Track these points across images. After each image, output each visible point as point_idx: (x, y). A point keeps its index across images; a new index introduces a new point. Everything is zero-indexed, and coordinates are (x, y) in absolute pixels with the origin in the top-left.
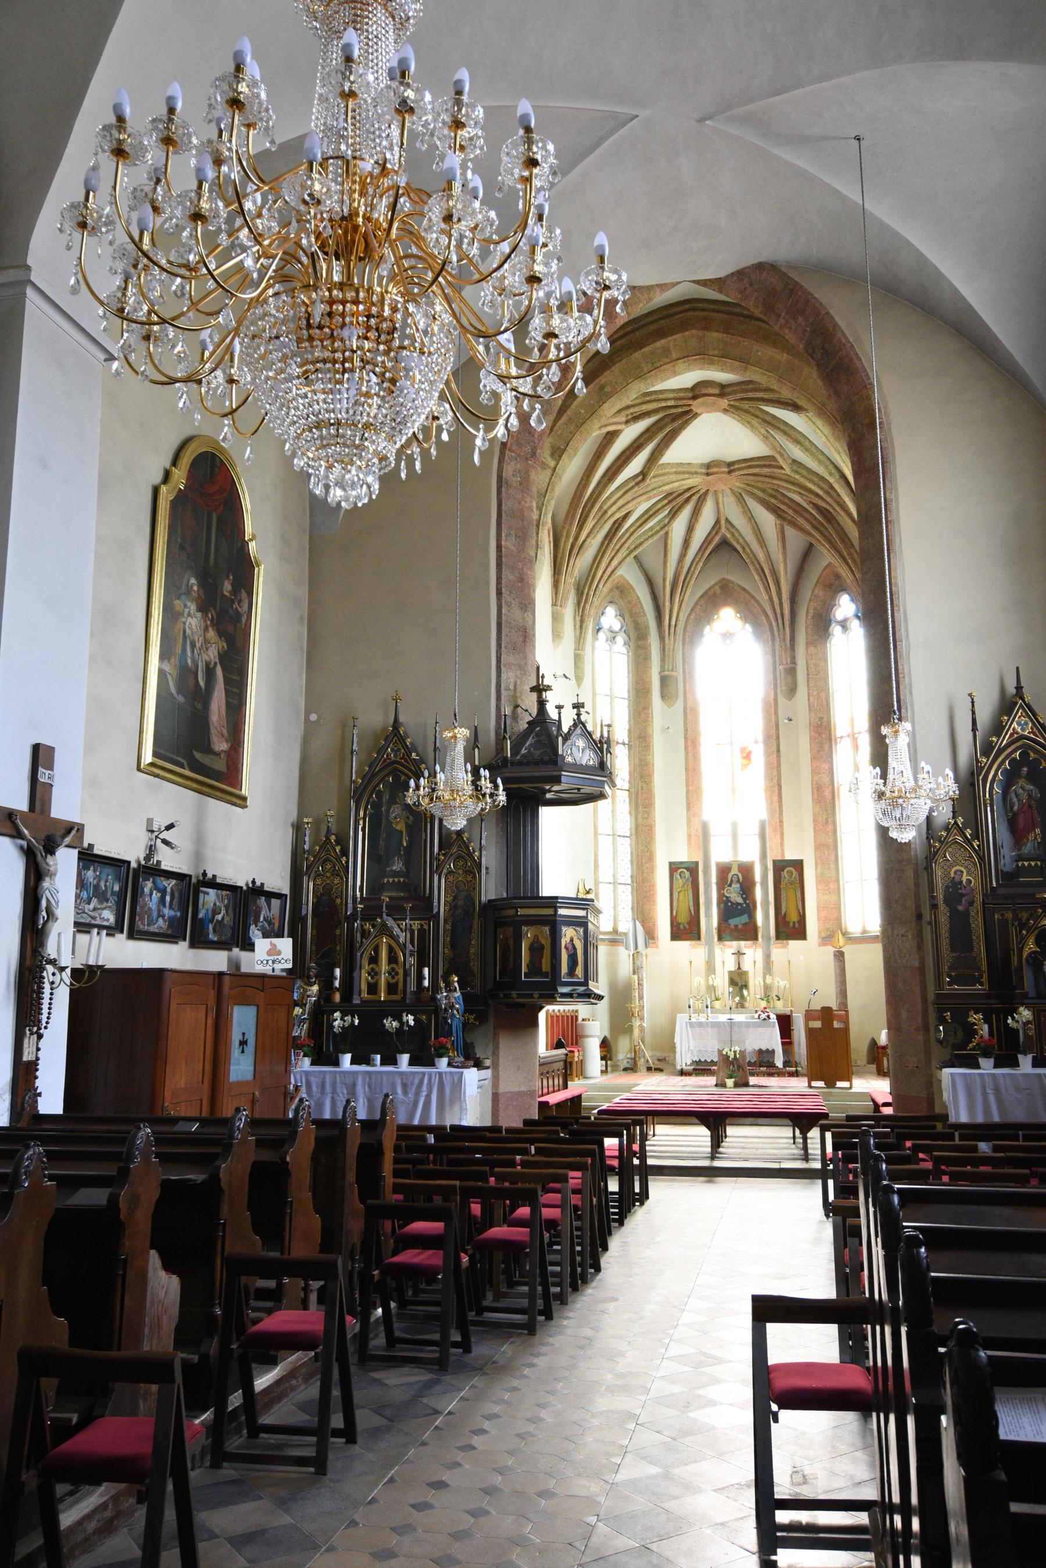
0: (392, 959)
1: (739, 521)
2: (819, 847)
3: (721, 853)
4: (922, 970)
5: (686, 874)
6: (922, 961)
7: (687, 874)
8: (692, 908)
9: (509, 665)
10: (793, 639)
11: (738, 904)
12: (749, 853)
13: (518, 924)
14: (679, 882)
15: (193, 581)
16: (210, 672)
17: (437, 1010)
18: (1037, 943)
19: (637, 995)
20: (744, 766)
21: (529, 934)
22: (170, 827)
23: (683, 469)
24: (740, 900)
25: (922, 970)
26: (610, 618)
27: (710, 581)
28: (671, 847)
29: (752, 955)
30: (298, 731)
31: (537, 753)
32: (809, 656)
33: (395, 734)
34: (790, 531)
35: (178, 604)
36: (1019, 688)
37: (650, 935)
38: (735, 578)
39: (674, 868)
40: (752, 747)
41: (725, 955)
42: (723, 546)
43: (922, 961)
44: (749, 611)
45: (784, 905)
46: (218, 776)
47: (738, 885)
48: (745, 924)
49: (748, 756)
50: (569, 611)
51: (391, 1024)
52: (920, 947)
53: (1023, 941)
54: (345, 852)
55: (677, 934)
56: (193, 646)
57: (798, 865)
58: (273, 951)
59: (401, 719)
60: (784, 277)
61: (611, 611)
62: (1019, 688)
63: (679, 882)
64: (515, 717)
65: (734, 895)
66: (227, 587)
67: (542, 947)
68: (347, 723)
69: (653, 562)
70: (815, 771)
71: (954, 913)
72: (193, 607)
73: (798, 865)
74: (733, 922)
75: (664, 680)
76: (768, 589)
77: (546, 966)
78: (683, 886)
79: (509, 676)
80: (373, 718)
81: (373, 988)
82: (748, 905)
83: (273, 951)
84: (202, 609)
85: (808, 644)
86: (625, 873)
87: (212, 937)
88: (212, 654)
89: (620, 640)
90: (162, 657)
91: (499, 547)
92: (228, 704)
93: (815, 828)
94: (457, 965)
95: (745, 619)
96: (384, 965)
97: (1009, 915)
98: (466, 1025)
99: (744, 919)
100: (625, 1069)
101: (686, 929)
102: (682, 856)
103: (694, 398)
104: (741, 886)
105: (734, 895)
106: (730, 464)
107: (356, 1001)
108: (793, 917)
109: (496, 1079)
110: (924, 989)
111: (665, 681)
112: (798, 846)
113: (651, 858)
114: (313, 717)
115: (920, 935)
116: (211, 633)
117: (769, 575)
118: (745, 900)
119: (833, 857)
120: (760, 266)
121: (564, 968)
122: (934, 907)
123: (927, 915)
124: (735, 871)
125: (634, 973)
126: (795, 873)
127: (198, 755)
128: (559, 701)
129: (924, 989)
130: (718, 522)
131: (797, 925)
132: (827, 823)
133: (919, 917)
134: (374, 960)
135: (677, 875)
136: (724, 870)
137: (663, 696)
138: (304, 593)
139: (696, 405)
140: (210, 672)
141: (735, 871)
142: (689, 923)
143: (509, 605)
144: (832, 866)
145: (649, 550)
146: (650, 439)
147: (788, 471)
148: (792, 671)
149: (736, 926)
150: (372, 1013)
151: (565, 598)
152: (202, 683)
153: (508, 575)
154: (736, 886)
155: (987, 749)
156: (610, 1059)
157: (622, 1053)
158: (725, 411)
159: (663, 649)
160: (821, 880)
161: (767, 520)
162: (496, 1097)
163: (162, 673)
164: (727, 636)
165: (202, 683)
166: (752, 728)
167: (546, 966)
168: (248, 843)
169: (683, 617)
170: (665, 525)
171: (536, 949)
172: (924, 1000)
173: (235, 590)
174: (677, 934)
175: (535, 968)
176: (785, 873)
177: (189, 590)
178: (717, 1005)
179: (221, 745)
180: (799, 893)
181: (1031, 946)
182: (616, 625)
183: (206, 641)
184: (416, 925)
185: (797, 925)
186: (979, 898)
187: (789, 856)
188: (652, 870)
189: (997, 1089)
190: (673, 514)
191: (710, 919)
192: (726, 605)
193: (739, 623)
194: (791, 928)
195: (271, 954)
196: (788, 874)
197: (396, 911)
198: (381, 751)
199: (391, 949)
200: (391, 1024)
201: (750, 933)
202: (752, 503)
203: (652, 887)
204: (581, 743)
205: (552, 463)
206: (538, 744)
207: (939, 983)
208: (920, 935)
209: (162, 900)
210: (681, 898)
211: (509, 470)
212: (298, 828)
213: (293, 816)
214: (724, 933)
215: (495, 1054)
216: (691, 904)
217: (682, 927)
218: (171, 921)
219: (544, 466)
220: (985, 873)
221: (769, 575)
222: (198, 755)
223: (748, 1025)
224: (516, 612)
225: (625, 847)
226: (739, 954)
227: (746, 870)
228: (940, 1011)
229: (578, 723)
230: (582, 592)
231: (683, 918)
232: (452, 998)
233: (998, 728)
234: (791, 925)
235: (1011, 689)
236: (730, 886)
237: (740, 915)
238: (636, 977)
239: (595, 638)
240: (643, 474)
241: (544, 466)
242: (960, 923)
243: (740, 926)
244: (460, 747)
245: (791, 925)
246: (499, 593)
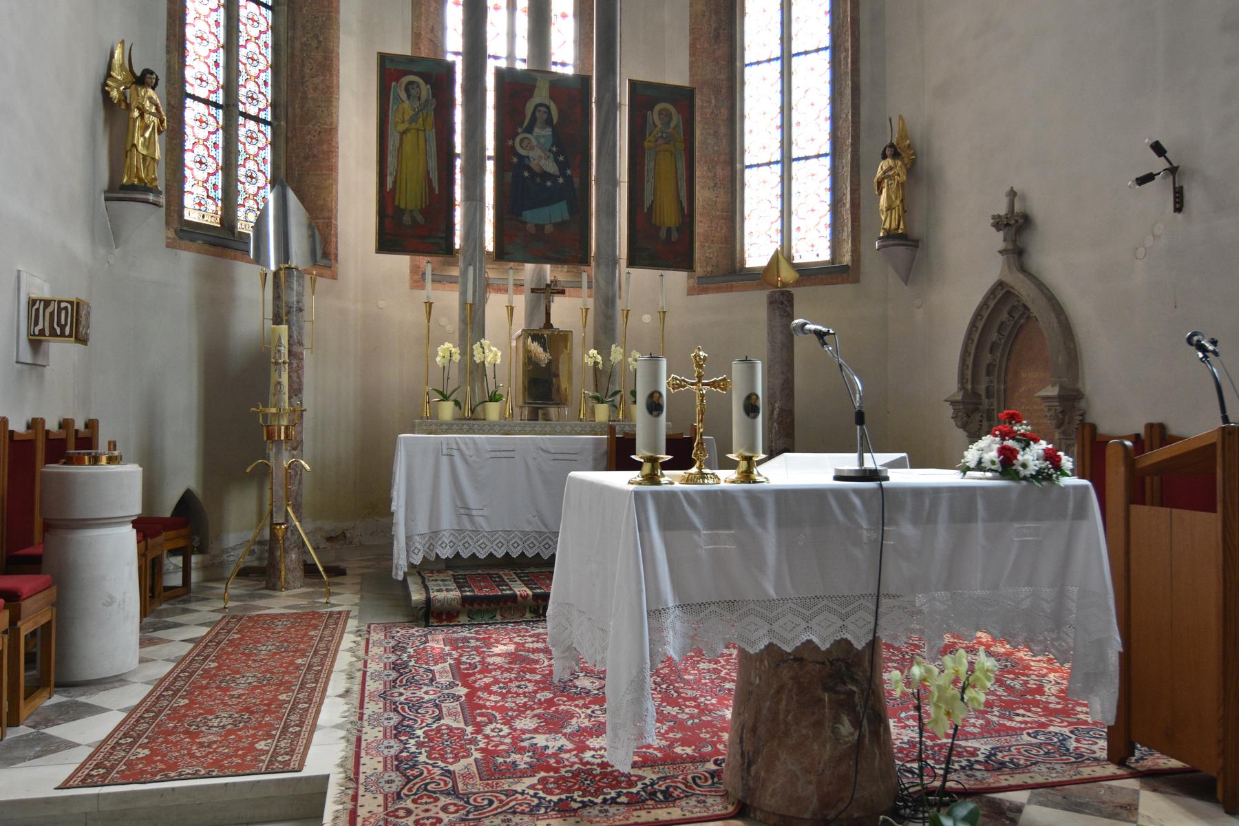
7: (425, 90)
8: (434, 176)
11: (546, 175)
14: (404, 108)
19: (285, 379)
24: (551, 168)
45: (648, 187)
47: (548, 132)
48: (560, 226)
63: (404, 108)
65: (539, 153)
74: (532, 217)
78: (413, 119)
82: (568, 179)
86: (256, 90)
93: (693, 46)
100: (244, 573)
104: (555, 134)
105: (539, 153)
108: (668, 217)
118: (562, 166)
119: (724, 112)
124: (541, 95)
125: (277, 320)
126: (676, 119)
131: (675, 236)
132: (717, 37)
135: (398, 89)
142: (423, 212)
144: (723, 130)
149: (540, 228)
154: (543, 133)
156: (202, 550)
176: (654, 116)
178: (493, 411)
180: (682, 165)
185: (675, 236)
191: (476, 212)
201: (568, 246)
203: (328, 133)
210: (408, 147)
216: (433, 164)
217: (406, 219)
226: (544, 293)
231: (411, 198)
234: (663, 234)
236: (529, 130)
237: (549, 201)
238: (284, 328)
243: (549, 229)
245: (663, 234)
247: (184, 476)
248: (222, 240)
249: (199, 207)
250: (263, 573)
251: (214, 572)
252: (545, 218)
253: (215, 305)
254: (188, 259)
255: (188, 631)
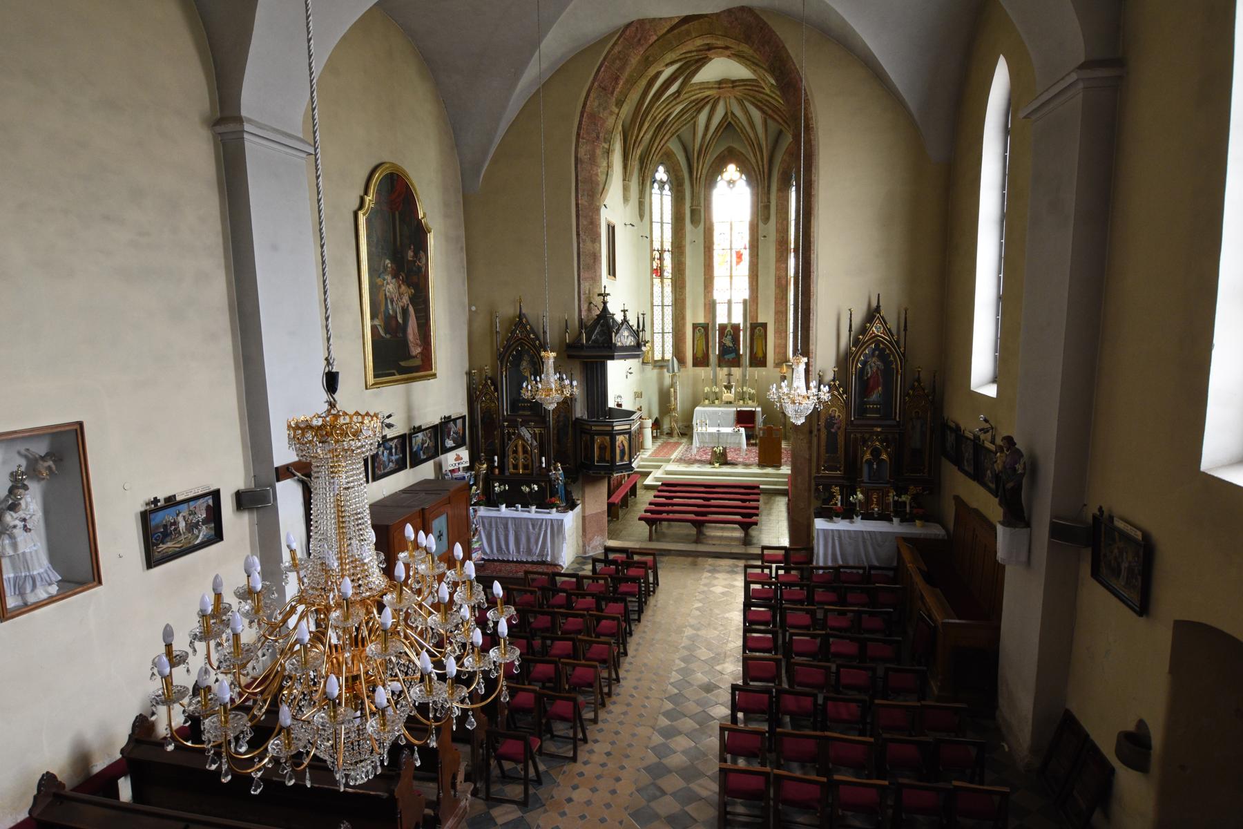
0: (525, 451)
1: (739, 113)
2: (777, 313)
3: (721, 319)
4: (810, 460)
5: (703, 330)
6: (811, 456)
9: (585, 279)
10: (769, 187)
12: (738, 319)
13: (592, 435)
15: (387, 261)
16: (405, 312)
17: (550, 480)
18: (871, 454)
20: (738, 263)
21: (598, 440)
22: (389, 416)
23: (704, 86)
25: (810, 460)
26: (661, 174)
27: (722, 148)
28: (695, 315)
29: (736, 371)
30: (464, 318)
31: (601, 339)
32: (778, 198)
33: (521, 316)
34: (770, 121)
35: (379, 281)
36: (878, 306)
37: (682, 361)
38: (736, 146)
39: (695, 326)
40: (743, 251)
41: (723, 372)
42: (728, 126)
43: (811, 456)
44: (744, 168)
46: (417, 369)
49: (739, 256)
50: (635, 164)
51: (526, 489)
52: (810, 448)
53: (864, 453)
54: (496, 389)
55: (695, 364)
56: (392, 301)
57: (764, 325)
58: (458, 458)
59: (524, 311)
60: (757, 17)
61: (661, 169)
62: (878, 306)
63: (698, 334)
64: (589, 310)
65: (729, 343)
66: (411, 253)
67: (605, 448)
68: (492, 314)
69: (687, 137)
70: (777, 269)
71: (829, 432)
72: (389, 278)
73: (764, 325)
75: (693, 212)
76: (755, 155)
77: (608, 457)
79: (585, 286)
80: (507, 311)
81: (516, 467)
83: (458, 458)
84: (395, 276)
85: (779, 190)
86: (669, 327)
87: (423, 457)
88: (406, 299)
89: (667, 187)
90: (372, 318)
91: (577, 205)
92: (419, 325)
94: (561, 457)
95: (742, 172)
96: (521, 455)
97: (859, 435)
98: (565, 484)
99: (733, 355)
101: (701, 361)
102: (701, 320)
103: (709, 49)
105: (729, 343)
106: (733, 82)
107: (507, 473)
108: (760, 355)
109: (583, 510)
110: (810, 470)
111: (694, 212)
112: (766, 316)
113: (683, 318)
114: (474, 308)
115: (810, 442)
116: (403, 287)
117: (755, 145)
120: (742, 9)
121: (618, 457)
122: (819, 430)
123: (815, 432)
124: (729, 329)
127: (402, 364)
128: (615, 308)
129: (810, 470)
130: (726, 114)
133: (811, 432)
134: (515, 452)
136: (723, 328)
137: (692, 221)
138: (462, 232)
139: (710, 54)
140: (405, 312)
141: (729, 329)
143: (584, 241)
145: (685, 132)
146: (681, 74)
147: (768, 91)
148: (767, 207)
150: (515, 482)
151: (631, 175)
152: (400, 320)
153: (583, 222)
155: (856, 342)
157: (666, 426)
158: (729, 57)
159: (693, 192)
160: (777, 331)
161: (756, 115)
162: (584, 518)
163: (374, 328)
164: (731, 183)
165: (400, 320)
166: (742, 239)
167: (608, 457)
168: (440, 396)
169: (704, 172)
170: (694, 118)
171: (602, 448)
172: (810, 476)
173: (416, 254)
174: (695, 364)
175: (601, 459)
177: (385, 268)
179: (416, 350)
181: (868, 456)
182: (665, 178)
183: (401, 295)
184: (537, 430)
186: (843, 425)
187: (760, 321)
188: (684, 325)
189: (840, 537)
190: (699, 111)
192: (731, 162)
193: (738, 174)
194: (758, 361)
195: (456, 459)
196: (758, 330)
197: (525, 423)
198: (513, 332)
199: (524, 447)
200: (526, 489)
201: (736, 362)
202: (747, 104)
204: (626, 333)
205: (617, 111)
206: (602, 333)
207: (818, 471)
208: (810, 442)
209: (391, 454)
211: (582, 151)
212: (469, 374)
213: (466, 367)
214: (722, 362)
215: (583, 497)
218: (397, 461)
219: (612, 113)
220: (848, 414)
221: (755, 145)
222: (402, 364)
223: (728, 434)
224: (589, 243)
225: (669, 311)
227: (736, 328)
228: (817, 485)
229: (625, 320)
230: (643, 161)
231: (700, 355)
232: (558, 473)
233: (863, 330)
235: (874, 304)
239: (652, 187)
240: (678, 92)
241: (612, 113)
242: (832, 438)
244: (551, 361)
246: (578, 234)
247: (656, 414)
248: (661, 364)
249: (658, 357)
250: (670, 434)
251: (662, 433)
252: (729, 356)
253: (661, 379)
254: (656, 371)
255: (659, 443)
